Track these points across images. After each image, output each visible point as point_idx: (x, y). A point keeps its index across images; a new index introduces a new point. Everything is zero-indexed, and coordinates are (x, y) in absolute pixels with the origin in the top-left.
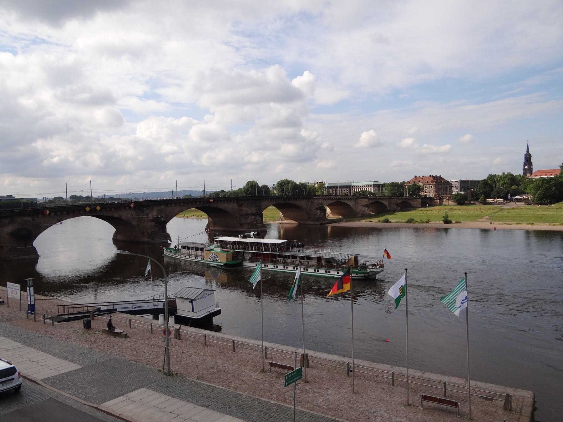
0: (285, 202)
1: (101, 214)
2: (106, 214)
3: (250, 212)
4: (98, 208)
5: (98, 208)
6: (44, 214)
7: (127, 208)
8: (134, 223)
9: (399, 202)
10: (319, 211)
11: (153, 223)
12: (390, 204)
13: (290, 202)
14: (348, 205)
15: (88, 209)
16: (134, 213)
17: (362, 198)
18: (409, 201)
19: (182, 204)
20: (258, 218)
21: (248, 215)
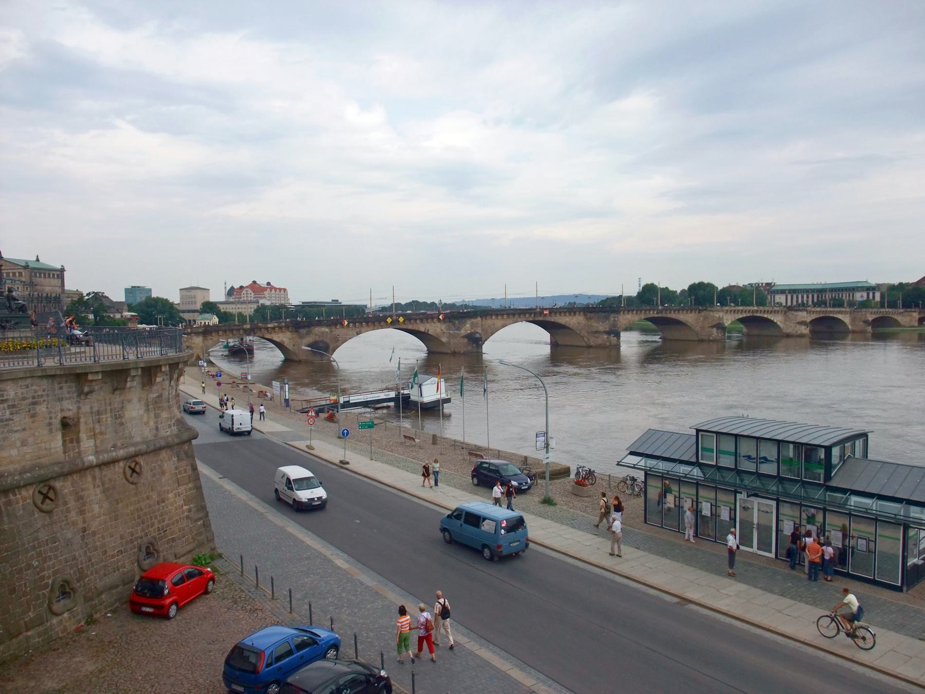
0: (660, 315)
1: (405, 327)
2: (410, 327)
3: (601, 328)
4: (401, 319)
5: (401, 319)
6: (342, 325)
7: (435, 320)
8: (444, 340)
9: (870, 318)
10: (715, 330)
11: (466, 340)
12: (853, 320)
13: (669, 316)
14: (772, 322)
15: (389, 320)
16: (443, 327)
17: (797, 310)
18: (895, 317)
19: (505, 316)
20: (613, 339)
21: (596, 332)
